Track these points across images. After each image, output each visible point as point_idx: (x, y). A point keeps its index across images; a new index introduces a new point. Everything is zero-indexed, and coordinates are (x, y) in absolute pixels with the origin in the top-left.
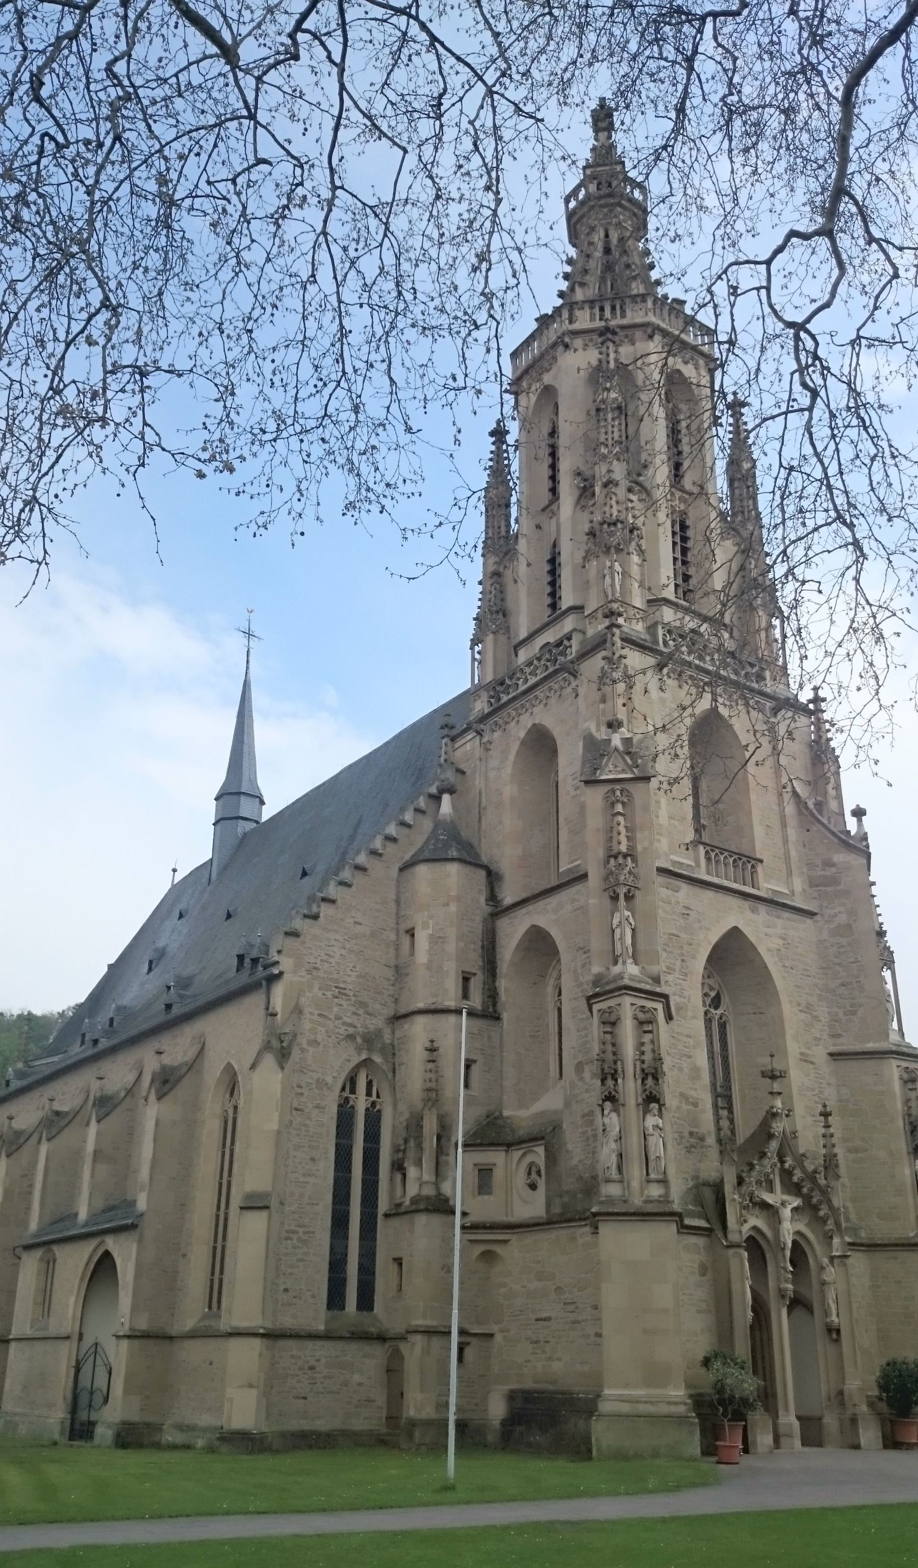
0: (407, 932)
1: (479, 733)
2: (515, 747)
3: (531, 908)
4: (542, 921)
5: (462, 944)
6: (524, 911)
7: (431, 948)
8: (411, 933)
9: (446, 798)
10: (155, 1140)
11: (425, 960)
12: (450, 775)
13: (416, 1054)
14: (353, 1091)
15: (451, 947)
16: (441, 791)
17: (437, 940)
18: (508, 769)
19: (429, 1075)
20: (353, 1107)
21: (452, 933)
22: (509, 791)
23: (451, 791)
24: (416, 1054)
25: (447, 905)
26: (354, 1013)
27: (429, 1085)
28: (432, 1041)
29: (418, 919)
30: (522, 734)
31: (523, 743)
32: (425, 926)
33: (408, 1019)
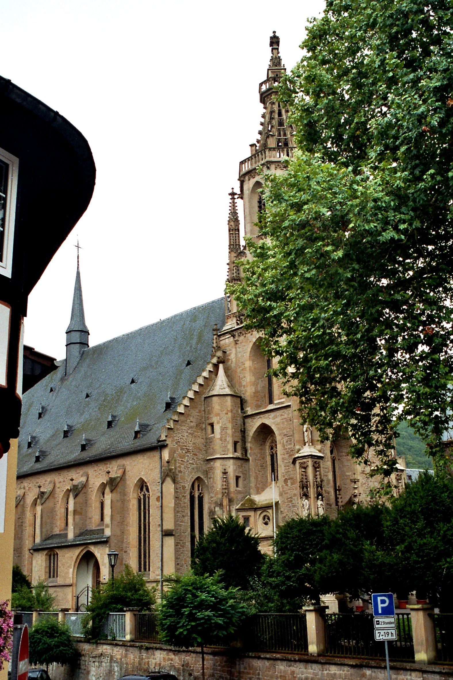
0: (209, 424)
1: (234, 336)
2: (251, 345)
3: (262, 416)
4: (267, 422)
5: (233, 430)
6: (258, 417)
7: (221, 432)
8: (212, 425)
9: (221, 366)
10: (111, 508)
11: (219, 437)
12: (219, 354)
13: (218, 474)
14: (193, 489)
15: (230, 432)
16: (219, 362)
17: (223, 429)
18: (248, 354)
19: (224, 483)
20: (193, 495)
21: (230, 426)
22: (248, 364)
23: (223, 362)
24: (218, 474)
25: (227, 414)
26: (193, 459)
27: (224, 487)
28: (225, 470)
29: (215, 420)
30: (254, 340)
31: (255, 343)
32: (218, 423)
33: (213, 461)
